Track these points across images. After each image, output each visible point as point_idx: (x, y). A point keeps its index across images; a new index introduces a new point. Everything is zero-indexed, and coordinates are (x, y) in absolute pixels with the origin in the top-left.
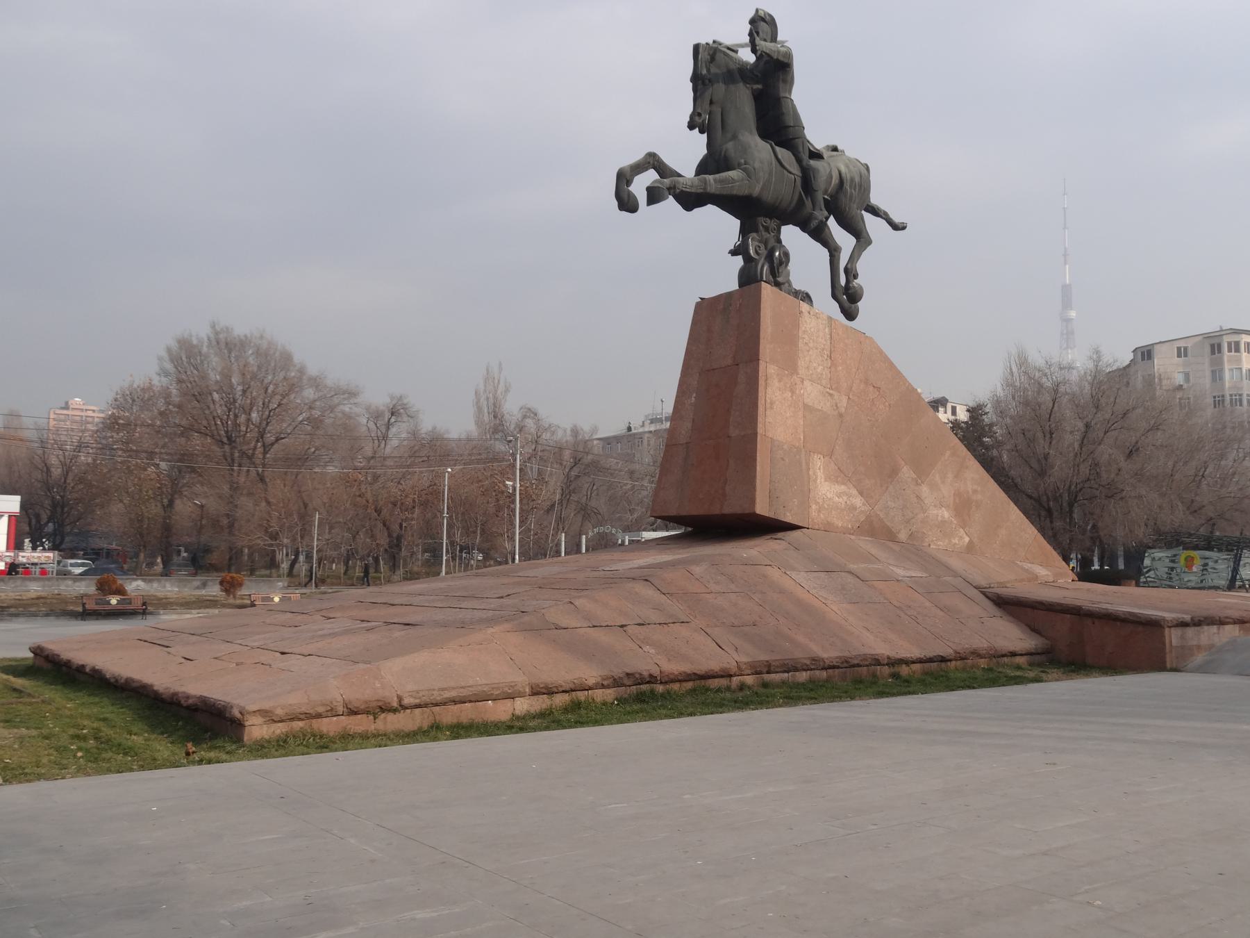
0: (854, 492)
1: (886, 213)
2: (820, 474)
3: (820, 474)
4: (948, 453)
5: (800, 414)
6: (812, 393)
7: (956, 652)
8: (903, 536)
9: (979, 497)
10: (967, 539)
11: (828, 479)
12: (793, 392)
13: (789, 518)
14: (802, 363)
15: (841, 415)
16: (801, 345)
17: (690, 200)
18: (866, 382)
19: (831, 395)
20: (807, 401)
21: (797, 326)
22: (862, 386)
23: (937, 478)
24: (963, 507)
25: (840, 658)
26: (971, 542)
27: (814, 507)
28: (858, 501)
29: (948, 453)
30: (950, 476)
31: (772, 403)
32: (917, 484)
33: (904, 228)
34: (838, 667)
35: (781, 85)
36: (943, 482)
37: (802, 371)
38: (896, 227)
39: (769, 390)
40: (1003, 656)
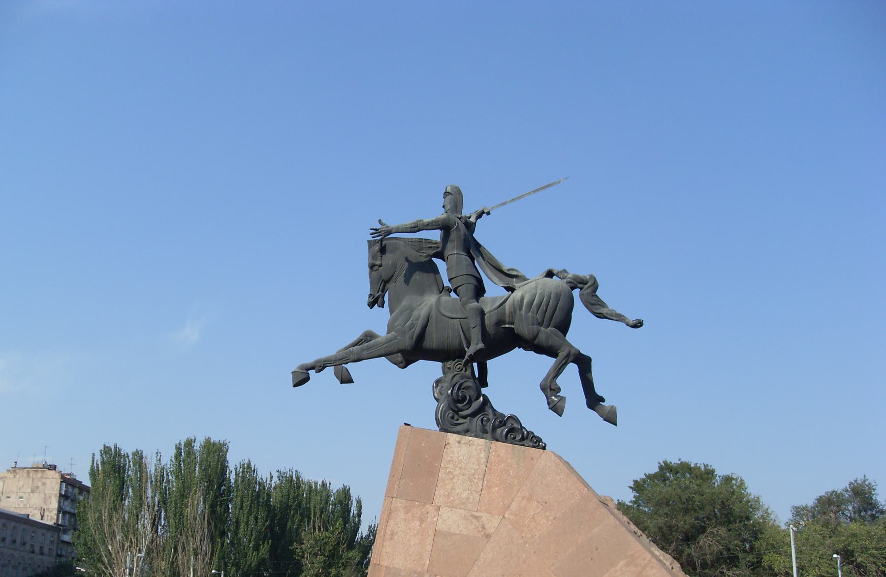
5: (430, 540)
6: (450, 520)
12: (422, 521)
14: (440, 493)
15: (488, 536)
16: (442, 475)
19: (477, 518)
20: (441, 526)
21: (439, 457)
22: (524, 503)
29: (622, 563)
31: (393, 534)
37: (438, 501)
39: (391, 522)
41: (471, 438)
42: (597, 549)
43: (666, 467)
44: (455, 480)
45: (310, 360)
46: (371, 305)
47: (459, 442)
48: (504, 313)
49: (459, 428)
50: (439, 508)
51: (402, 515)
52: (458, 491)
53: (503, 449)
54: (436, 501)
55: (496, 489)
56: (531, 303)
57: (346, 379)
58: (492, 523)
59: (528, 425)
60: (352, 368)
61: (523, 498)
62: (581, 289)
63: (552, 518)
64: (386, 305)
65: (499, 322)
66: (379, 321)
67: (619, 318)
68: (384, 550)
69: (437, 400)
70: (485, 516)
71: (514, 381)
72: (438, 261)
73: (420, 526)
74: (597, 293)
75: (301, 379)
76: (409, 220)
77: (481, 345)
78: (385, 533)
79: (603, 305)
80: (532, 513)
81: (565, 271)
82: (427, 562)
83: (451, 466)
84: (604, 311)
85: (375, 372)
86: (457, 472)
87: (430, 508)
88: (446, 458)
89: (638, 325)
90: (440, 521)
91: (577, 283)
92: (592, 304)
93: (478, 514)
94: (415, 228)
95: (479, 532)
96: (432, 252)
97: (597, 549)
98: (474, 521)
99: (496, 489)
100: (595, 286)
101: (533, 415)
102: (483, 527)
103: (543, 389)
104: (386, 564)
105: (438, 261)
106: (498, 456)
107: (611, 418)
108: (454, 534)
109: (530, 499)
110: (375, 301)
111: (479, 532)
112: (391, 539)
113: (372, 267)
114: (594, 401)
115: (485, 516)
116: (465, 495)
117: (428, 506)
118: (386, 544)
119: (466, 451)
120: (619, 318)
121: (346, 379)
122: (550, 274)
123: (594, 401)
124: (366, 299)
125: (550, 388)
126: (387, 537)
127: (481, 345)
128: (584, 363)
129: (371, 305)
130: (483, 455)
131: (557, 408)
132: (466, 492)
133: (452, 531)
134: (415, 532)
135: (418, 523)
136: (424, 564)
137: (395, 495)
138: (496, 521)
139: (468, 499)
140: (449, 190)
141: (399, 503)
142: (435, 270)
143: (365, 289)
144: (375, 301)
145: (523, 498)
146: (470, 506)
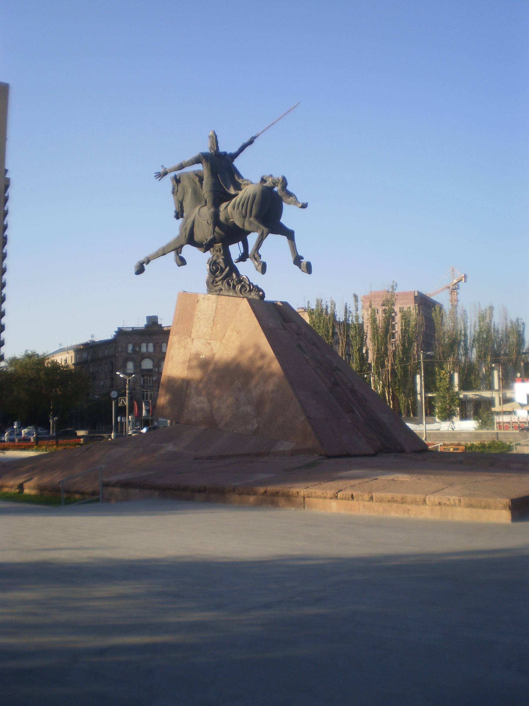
10: (256, 425)
12: (185, 348)
14: (194, 330)
16: (195, 320)
19: (209, 344)
26: (258, 427)
27: (186, 411)
31: (172, 357)
43: (285, 304)
47: (204, 299)
54: (192, 335)
70: (213, 343)
76: (176, 163)
81: (271, 176)
87: (189, 340)
89: (304, 206)
94: (181, 167)
102: (212, 350)
115: (213, 343)
116: (205, 331)
124: (174, 214)
128: (290, 235)
130: (214, 305)
135: (183, 349)
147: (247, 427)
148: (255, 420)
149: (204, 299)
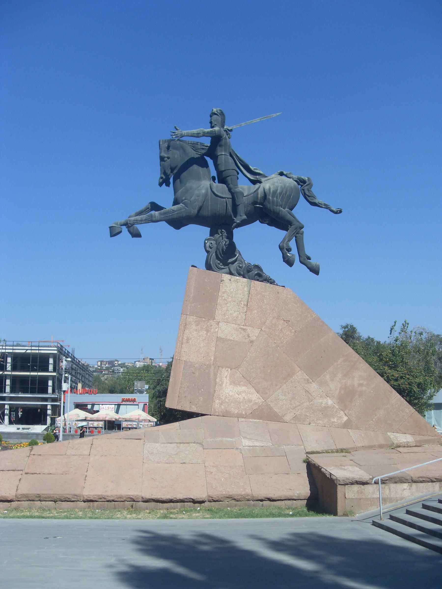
0: (253, 390)
1: (325, 205)
2: (226, 381)
3: (226, 381)
4: (341, 360)
5: (213, 344)
6: (227, 330)
7: (209, 496)
8: (288, 418)
9: (364, 388)
10: (345, 418)
11: (234, 383)
12: (208, 331)
13: (194, 409)
15: (252, 342)
17: (177, 223)
18: (278, 318)
19: (244, 329)
20: (220, 335)
21: (217, 289)
23: (328, 377)
24: (346, 397)
25: (99, 496)
26: (349, 420)
27: (217, 401)
28: (255, 397)
29: (341, 360)
30: (340, 375)
31: (188, 339)
32: (308, 382)
33: (341, 212)
34: (97, 501)
35: (219, 148)
36: (332, 380)
37: (218, 317)
38: (336, 213)
39: (187, 332)
40: (262, 500)
41: (238, 278)
42: (324, 351)
44: (228, 305)
45: (123, 221)
46: (161, 184)
47: (230, 280)
48: (257, 197)
49: (223, 270)
50: (218, 323)
51: (194, 327)
52: (231, 312)
53: (258, 285)
54: (217, 318)
55: (256, 311)
56: (275, 192)
57: (136, 235)
58: (254, 333)
59: (267, 272)
60: (141, 228)
61: (274, 318)
62: (302, 186)
63: (293, 331)
64: (171, 185)
65: (255, 203)
66: (165, 197)
67: (327, 207)
68: (182, 350)
69: (208, 252)
70: (249, 329)
71: (256, 241)
72: (208, 159)
73: (207, 334)
74: (312, 189)
75: (114, 232)
77: (245, 217)
78: (183, 338)
79: (314, 197)
80: (280, 328)
82: (213, 358)
83: (225, 295)
84: (316, 201)
85: (158, 232)
86: (230, 300)
88: (222, 290)
90: (220, 331)
91: (301, 182)
92: (309, 196)
93: (245, 327)
94: (197, 136)
95: (246, 339)
96: (204, 152)
97: (324, 351)
98: (242, 332)
99: (256, 311)
100: (310, 185)
101: (272, 265)
102: (249, 336)
103: (281, 248)
104: (184, 359)
105: (208, 159)
106: (256, 290)
107: (315, 271)
108: (229, 340)
109: (278, 318)
110: (165, 181)
111: (246, 339)
112: (187, 342)
113: (162, 159)
114: (305, 260)
116: (235, 315)
117: (211, 321)
118: (184, 346)
119: (233, 287)
120: (327, 207)
121: (136, 235)
122: (281, 174)
123: (305, 260)
125: (284, 249)
126: (184, 341)
127: (245, 217)
129: (161, 184)
130: (246, 289)
131: (290, 263)
132: (236, 313)
133: (228, 338)
134: (203, 338)
135: (205, 332)
136: (211, 359)
137: (188, 314)
138: (257, 332)
139: (237, 317)
140: (215, 110)
141: (191, 319)
142: (205, 165)
143: (157, 175)
144: (165, 181)
145: (274, 318)
146: (239, 322)
147: (332, 420)
148: (342, 412)
149: (230, 280)
